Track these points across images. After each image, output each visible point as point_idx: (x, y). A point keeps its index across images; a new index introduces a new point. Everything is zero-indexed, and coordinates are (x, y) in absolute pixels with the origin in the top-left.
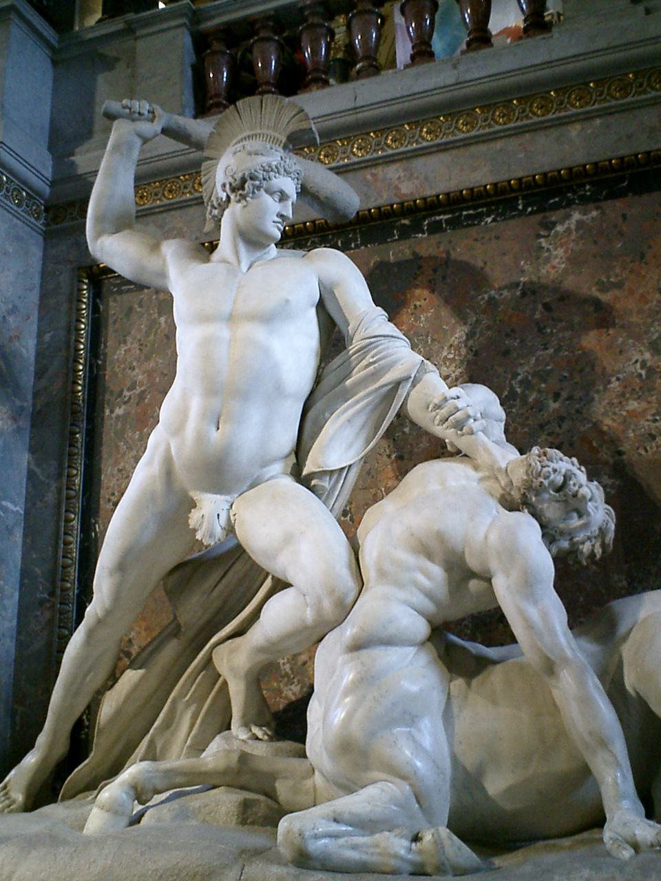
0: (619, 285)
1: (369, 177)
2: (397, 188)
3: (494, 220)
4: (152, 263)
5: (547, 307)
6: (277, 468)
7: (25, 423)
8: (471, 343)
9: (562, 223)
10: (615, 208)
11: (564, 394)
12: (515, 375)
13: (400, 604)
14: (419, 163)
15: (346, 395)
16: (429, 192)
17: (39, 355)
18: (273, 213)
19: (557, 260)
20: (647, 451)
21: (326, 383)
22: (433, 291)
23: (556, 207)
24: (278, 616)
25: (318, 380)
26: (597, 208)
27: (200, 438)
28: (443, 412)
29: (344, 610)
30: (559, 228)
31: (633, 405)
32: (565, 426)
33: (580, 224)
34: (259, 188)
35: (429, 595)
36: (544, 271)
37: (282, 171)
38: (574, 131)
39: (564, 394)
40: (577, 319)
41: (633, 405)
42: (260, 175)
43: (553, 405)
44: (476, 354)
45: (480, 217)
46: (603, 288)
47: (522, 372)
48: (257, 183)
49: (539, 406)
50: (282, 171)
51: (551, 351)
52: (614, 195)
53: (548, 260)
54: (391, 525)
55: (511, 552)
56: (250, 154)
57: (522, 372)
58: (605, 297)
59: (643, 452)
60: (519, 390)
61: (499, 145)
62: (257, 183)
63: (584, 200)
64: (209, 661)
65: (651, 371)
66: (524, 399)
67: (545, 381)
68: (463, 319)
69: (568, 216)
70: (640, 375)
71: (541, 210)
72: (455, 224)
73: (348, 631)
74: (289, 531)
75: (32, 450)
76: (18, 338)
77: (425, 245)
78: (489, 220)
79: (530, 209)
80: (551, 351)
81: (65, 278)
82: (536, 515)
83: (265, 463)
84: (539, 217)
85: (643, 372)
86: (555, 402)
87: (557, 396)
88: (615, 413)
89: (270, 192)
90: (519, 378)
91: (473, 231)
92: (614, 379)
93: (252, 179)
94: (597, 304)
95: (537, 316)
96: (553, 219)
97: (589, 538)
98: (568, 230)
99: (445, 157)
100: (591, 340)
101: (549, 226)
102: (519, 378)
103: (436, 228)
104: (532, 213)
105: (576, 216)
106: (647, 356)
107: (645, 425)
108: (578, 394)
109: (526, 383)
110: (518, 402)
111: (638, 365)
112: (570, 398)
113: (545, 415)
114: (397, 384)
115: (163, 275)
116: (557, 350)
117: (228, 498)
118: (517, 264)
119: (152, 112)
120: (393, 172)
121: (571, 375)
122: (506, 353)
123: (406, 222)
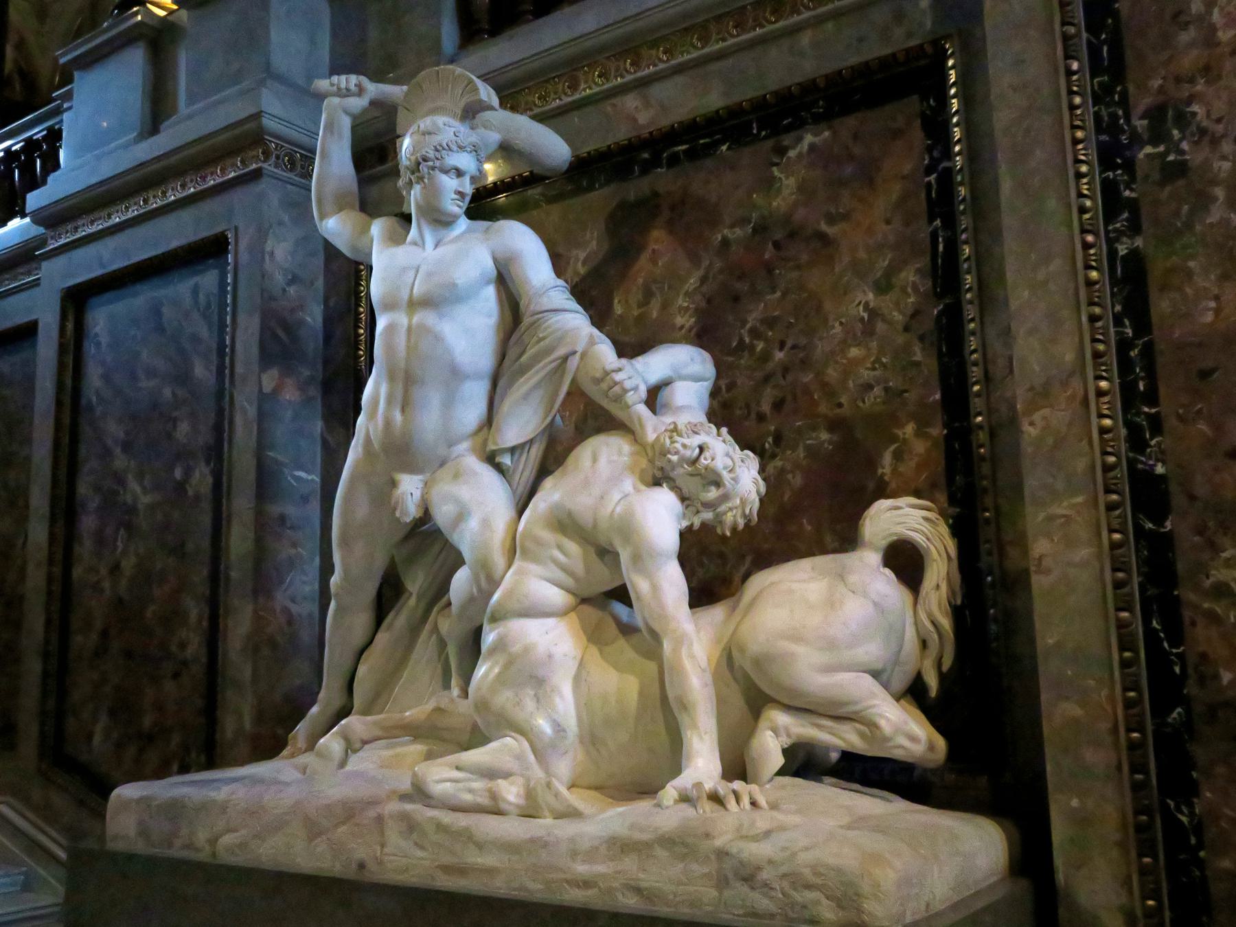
0: (846, 217)
1: (609, 109)
2: (635, 120)
3: (729, 149)
5: (777, 245)
6: (465, 445)
7: (315, 392)
8: (704, 289)
9: (793, 148)
11: (789, 344)
12: (744, 322)
14: (659, 91)
15: (523, 371)
16: (665, 122)
17: (328, 321)
19: (788, 191)
20: (864, 402)
22: (671, 232)
23: (788, 129)
25: (502, 356)
26: (830, 128)
27: (388, 423)
28: (604, 386)
30: (792, 153)
31: (854, 352)
32: (789, 378)
33: (812, 147)
34: (433, 168)
35: (564, 569)
36: (775, 204)
37: (454, 148)
38: (805, 39)
39: (789, 344)
40: (804, 257)
41: (854, 352)
42: (431, 154)
43: (779, 355)
44: (709, 301)
45: (716, 145)
46: (831, 219)
47: (753, 319)
48: (430, 163)
49: (766, 357)
50: (454, 148)
51: (778, 294)
52: (846, 111)
53: (779, 190)
56: (424, 134)
57: (753, 319)
58: (830, 231)
59: (861, 404)
60: (747, 340)
61: (729, 62)
62: (430, 163)
63: (818, 119)
64: (436, 629)
65: (874, 313)
66: (752, 348)
67: (771, 329)
68: (695, 259)
69: (800, 139)
70: (863, 318)
72: (694, 155)
74: (478, 506)
75: (326, 419)
76: (302, 307)
77: (663, 180)
78: (724, 148)
79: (764, 133)
80: (778, 294)
82: (675, 488)
83: (451, 444)
84: (770, 143)
85: (866, 316)
86: (781, 349)
87: (782, 346)
88: (837, 362)
89: (446, 172)
90: (748, 326)
91: (709, 163)
92: (837, 324)
93: (425, 160)
94: (822, 237)
95: (767, 256)
96: (786, 143)
97: (731, 509)
98: (800, 155)
99: (679, 79)
100: (816, 279)
101: (781, 151)
102: (748, 326)
103: (674, 161)
104: (766, 138)
105: (809, 138)
106: (871, 296)
107: (866, 374)
108: (803, 341)
109: (755, 334)
110: (746, 354)
111: (861, 308)
112: (794, 347)
113: (770, 366)
114: (565, 359)
116: (784, 294)
117: (420, 477)
118: (750, 196)
119: (359, 86)
120: (631, 102)
121: (796, 320)
122: (736, 299)
123: (646, 155)
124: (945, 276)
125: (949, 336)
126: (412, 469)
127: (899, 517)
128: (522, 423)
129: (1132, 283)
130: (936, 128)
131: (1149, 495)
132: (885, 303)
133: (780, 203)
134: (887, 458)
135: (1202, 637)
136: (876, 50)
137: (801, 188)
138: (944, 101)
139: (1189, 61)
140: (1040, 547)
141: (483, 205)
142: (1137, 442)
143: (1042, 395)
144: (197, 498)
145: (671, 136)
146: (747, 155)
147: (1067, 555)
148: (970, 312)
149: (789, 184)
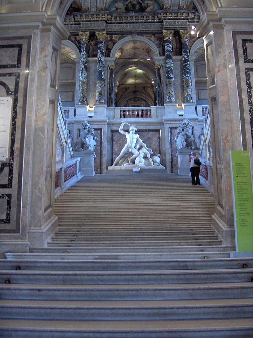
4: (125, 133)
10: (154, 132)
13: (142, 155)
18: (134, 132)
21: (137, 142)
24: (134, 156)
29: (139, 155)
38: (152, 126)
52: (154, 131)
54: (141, 151)
55: (148, 153)
71: (149, 131)
72: (143, 131)
73: (139, 156)
81: (109, 131)
115: (126, 134)
124: (160, 142)
125: (160, 146)
126: (130, 148)
127: (159, 155)
128: (138, 147)
129: (171, 145)
130: (159, 134)
131: (172, 155)
132: (156, 144)
133: (149, 136)
134: (156, 153)
135: (173, 161)
136: (156, 129)
137: (151, 136)
138: (160, 133)
139: (175, 135)
140: (167, 157)
141: (136, 132)
142: (171, 152)
143: (167, 149)
144: (98, 149)
145: (141, 130)
146: (147, 133)
147: (168, 158)
148: (161, 145)
149: (150, 135)
